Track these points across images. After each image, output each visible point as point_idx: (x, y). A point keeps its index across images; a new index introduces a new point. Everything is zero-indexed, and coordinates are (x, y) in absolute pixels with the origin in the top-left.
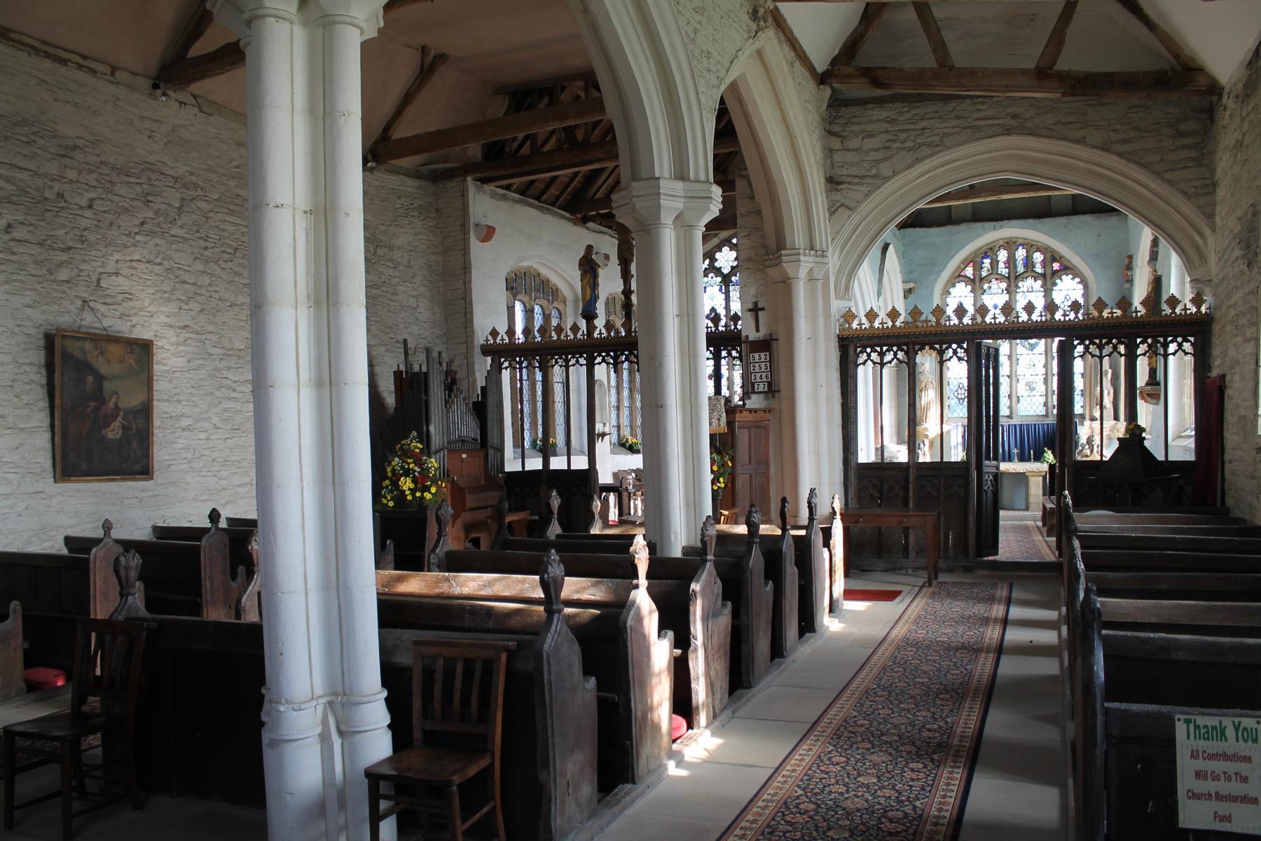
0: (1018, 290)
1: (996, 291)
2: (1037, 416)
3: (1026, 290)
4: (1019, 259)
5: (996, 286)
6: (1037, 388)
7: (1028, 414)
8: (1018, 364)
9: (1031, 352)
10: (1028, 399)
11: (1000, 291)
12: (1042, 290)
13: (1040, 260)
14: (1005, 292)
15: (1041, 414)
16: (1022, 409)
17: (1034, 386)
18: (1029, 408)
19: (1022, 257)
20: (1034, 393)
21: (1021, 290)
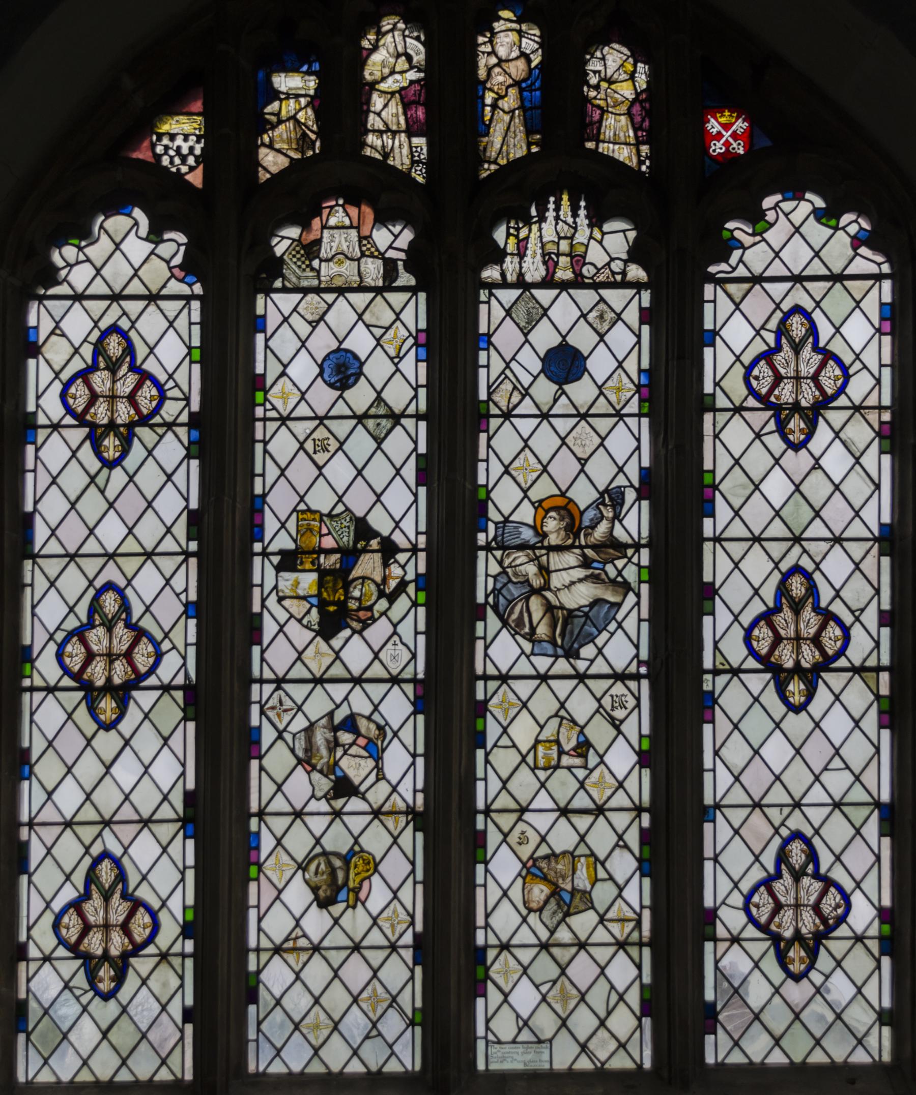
0: (491, 273)
1: (347, 271)
2: (601, 1074)
3: (534, 270)
4: (499, 78)
5: (347, 241)
6: (603, 894)
7: (539, 1060)
8: (480, 740)
9: (562, 666)
10: (545, 968)
11: (373, 270)
12: (636, 272)
13: (626, 91)
14: (405, 279)
15: (621, 1062)
16: (504, 1026)
17: (582, 880)
18: (546, 1023)
19: (518, 69)
20: (584, 922)
21: (510, 265)
